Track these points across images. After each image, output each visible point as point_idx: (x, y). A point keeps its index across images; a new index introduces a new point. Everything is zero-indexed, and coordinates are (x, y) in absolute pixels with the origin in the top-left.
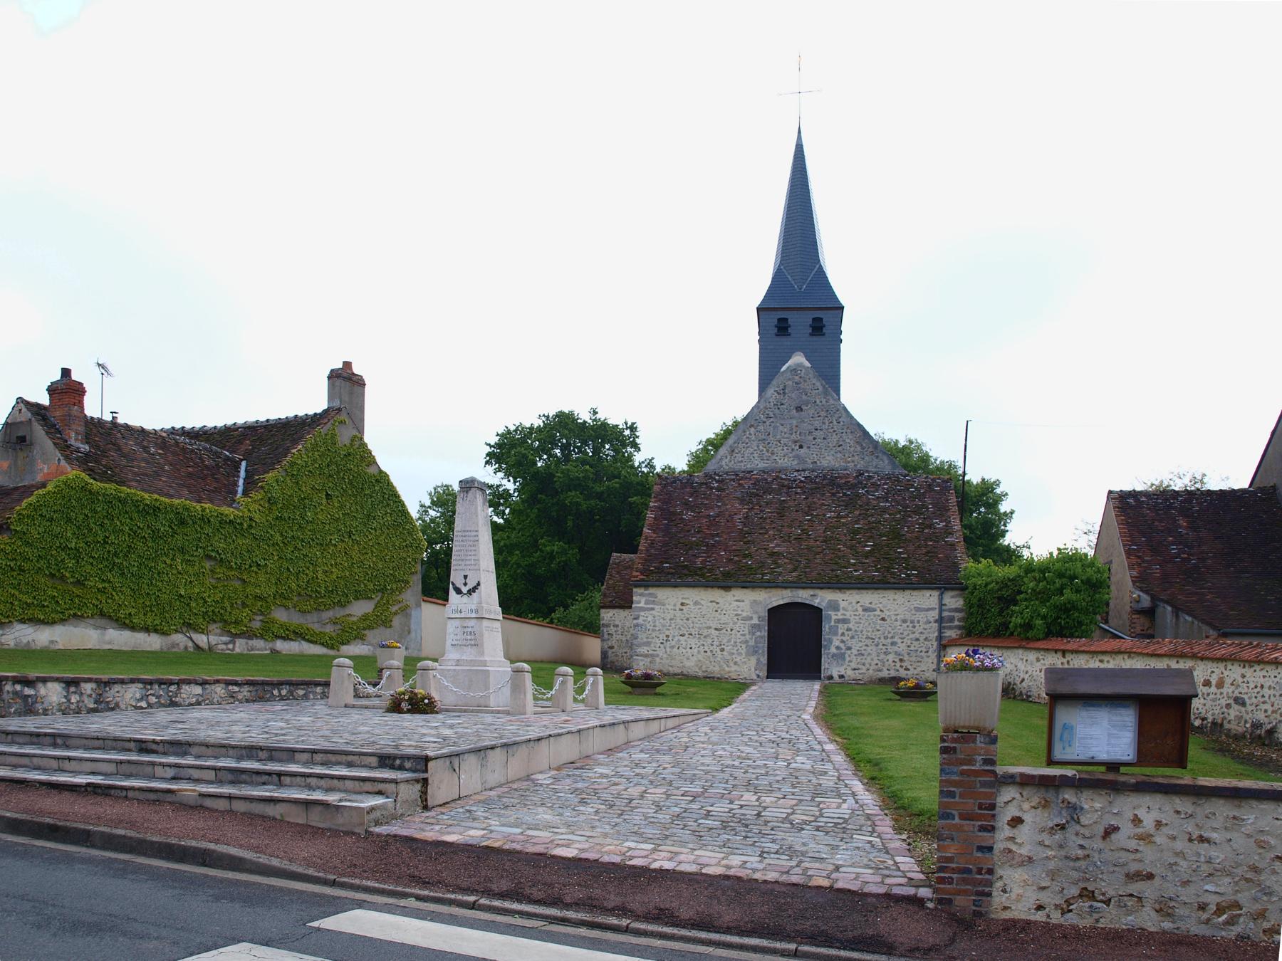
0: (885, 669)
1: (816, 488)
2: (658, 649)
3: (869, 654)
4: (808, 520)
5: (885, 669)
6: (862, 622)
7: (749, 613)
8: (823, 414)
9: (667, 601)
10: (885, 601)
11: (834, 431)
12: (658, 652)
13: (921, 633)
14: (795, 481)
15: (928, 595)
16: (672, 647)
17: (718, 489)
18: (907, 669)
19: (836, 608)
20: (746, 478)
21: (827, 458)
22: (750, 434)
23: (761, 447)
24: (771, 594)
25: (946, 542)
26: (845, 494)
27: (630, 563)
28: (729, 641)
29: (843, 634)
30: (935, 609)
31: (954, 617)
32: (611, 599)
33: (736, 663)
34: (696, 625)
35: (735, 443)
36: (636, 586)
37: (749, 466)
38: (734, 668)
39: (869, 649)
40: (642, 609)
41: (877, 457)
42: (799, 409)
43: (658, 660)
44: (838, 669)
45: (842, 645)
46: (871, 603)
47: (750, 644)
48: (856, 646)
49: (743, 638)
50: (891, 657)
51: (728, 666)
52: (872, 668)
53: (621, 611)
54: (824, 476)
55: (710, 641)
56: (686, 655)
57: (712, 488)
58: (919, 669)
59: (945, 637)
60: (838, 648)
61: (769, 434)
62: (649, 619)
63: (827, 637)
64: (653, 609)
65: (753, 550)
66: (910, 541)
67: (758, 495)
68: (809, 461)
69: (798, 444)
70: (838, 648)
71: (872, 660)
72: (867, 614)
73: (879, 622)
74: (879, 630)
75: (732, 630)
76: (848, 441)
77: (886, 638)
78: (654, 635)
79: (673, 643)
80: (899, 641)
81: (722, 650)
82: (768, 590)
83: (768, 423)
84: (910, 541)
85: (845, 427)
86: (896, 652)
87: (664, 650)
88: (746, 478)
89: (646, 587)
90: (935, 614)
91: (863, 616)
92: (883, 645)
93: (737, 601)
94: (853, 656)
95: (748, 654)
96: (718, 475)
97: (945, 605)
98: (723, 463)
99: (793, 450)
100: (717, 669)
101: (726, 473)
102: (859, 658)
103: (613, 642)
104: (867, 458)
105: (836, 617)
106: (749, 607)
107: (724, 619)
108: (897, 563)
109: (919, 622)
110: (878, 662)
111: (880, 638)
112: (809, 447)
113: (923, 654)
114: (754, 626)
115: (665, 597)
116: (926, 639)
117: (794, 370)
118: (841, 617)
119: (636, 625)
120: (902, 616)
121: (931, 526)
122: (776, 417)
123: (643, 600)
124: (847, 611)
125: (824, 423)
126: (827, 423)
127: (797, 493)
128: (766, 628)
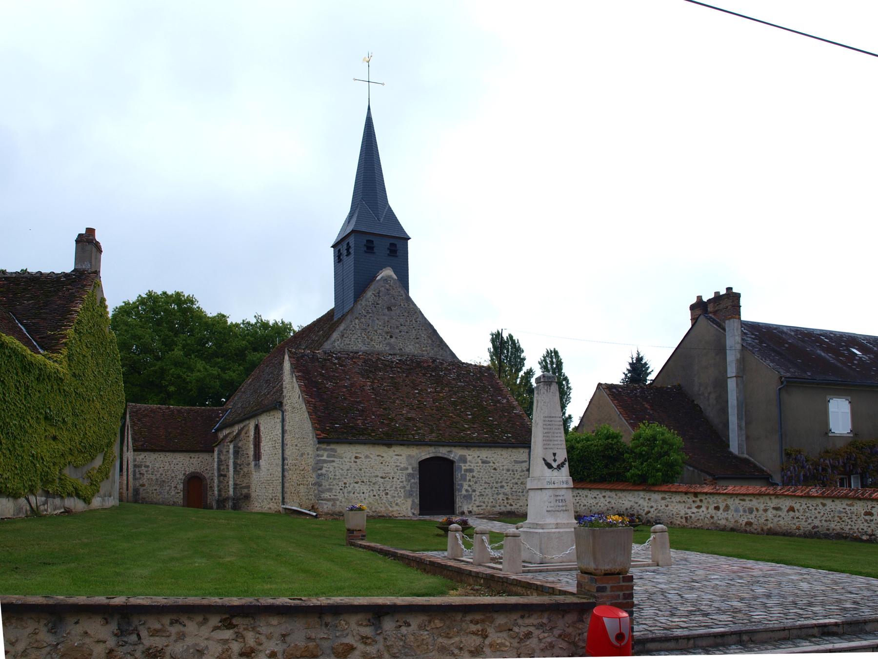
0: (497, 505)
3: (487, 495)
5: (497, 505)
6: (482, 471)
7: (405, 465)
10: (496, 456)
11: (414, 328)
12: (338, 497)
13: (519, 479)
15: (522, 452)
16: (349, 492)
18: (511, 505)
19: (465, 461)
21: (409, 347)
22: (355, 324)
23: (363, 334)
24: (421, 450)
27: (146, 412)
28: (392, 487)
29: (470, 480)
30: (525, 462)
32: (141, 443)
33: (397, 504)
34: (367, 474)
35: (344, 330)
37: (354, 348)
38: (396, 508)
39: (487, 491)
41: (442, 349)
42: (389, 309)
43: (338, 503)
45: (469, 489)
46: (487, 458)
47: (407, 489)
48: (479, 489)
50: (501, 497)
51: (391, 506)
52: (489, 505)
53: (152, 454)
55: (377, 487)
56: (360, 499)
58: (518, 505)
60: (467, 491)
61: (369, 326)
64: (333, 461)
68: (397, 348)
70: (467, 491)
71: (489, 499)
72: (485, 465)
73: (493, 471)
74: (492, 477)
75: (393, 478)
76: (423, 335)
77: (497, 483)
78: (334, 482)
79: (350, 489)
80: (505, 485)
81: (387, 494)
82: (419, 447)
83: (368, 317)
85: (421, 325)
89: (329, 443)
91: (482, 466)
92: (496, 488)
93: (396, 455)
95: (406, 497)
98: (336, 344)
99: (385, 338)
100: (383, 509)
101: (339, 352)
103: (144, 480)
104: (435, 349)
106: (405, 459)
107: (387, 469)
109: (517, 471)
110: (492, 500)
111: (493, 483)
112: (396, 338)
113: (520, 494)
114: (409, 475)
115: (342, 452)
117: (386, 280)
118: (468, 468)
119: (322, 475)
120: (507, 467)
121: (499, 401)
123: (326, 454)
124: (472, 463)
125: (406, 321)
127: (399, 372)
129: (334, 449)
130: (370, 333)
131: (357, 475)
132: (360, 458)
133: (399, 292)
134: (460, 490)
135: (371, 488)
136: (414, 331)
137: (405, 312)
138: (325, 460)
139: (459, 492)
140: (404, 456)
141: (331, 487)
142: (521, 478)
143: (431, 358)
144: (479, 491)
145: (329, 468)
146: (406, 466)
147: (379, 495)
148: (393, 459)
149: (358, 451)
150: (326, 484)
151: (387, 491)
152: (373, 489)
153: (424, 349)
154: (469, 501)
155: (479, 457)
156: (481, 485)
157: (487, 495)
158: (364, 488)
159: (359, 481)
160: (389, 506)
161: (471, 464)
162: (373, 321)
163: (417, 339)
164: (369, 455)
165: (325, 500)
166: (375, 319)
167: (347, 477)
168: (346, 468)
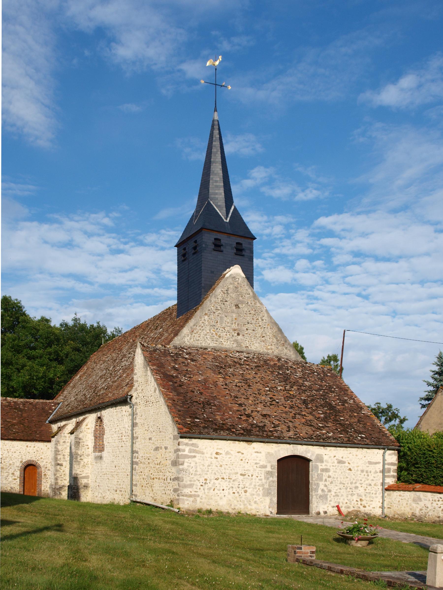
0: (351, 506)
3: (342, 495)
9: (205, 451)
11: (260, 326)
13: (373, 480)
14: (240, 359)
16: (209, 489)
17: (192, 360)
18: (365, 507)
20: (206, 354)
21: (255, 345)
22: (204, 320)
23: (212, 331)
28: (251, 484)
29: (326, 480)
30: (379, 463)
31: (390, 468)
33: (255, 502)
34: (226, 471)
35: (194, 325)
37: (203, 344)
39: (342, 491)
40: (186, 457)
41: (286, 348)
42: (237, 306)
43: (198, 499)
44: (323, 506)
45: (325, 489)
48: (334, 489)
51: (250, 504)
55: (236, 483)
56: (220, 495)
57: (186, 358)
58: (371, 506)
59: (386, 483)
61: (217, 322)
63: (316, 482)
64: (195, 457)
67: (221, 367)
68: (244, 346)
69: (236, 332)
70: (323, 490)
71: (344, 499)
72: (340, 465)
74: (347, 478)
75: (252, 476)
76: (268, 334)
77: (351, 483)
78: (195, 478)
79: (210, 485)
80: (359, 486)
81: (246, 492)
83: (216, 314)
86: (358, 494)
87: (203, 491)
90: (380, 467)
92: (350, 489)
94: (332, 497)
95: (264, 495)
102: (336, 498)
104: (280, 348)
107: (247, 466)
109: (370, 472)
112: (243, 335)
113: (373, 495)
114: (268, 473)
116: (375, 485)
117: (233, 277)
118: (324, 467)
121: (345, 401)
122: (222, 310)
123: (187, 449)
126: (255, 319)
127: (247, 369)
128: (276, 474)
129: (195, 444)
130: (218, 330)
131: (217, 471)
132: (221, 454)
133: (247, 290)
134: (316, 490)
135: (231, 485)
136: (260, 329)
137: (252, 310)
140: (263, 454)
141: (192, 482)
143: (277, 357)
145: (190, 463)
146: (265, 464)
147: (238, 492)
149: (219, 447)
150: (187, 480)
151: (246, 489)
152: (233, 486)
153: (269, 347)
154: (324, 501)
156: (336, 486)
157: (342, 495)
158: (224, 484)
160: (248, 504)
162: (221, 318)
164: (230, 451)
165: (186, 496)
166: (223, 316)
167: (208, 473)
168: (207, 464)
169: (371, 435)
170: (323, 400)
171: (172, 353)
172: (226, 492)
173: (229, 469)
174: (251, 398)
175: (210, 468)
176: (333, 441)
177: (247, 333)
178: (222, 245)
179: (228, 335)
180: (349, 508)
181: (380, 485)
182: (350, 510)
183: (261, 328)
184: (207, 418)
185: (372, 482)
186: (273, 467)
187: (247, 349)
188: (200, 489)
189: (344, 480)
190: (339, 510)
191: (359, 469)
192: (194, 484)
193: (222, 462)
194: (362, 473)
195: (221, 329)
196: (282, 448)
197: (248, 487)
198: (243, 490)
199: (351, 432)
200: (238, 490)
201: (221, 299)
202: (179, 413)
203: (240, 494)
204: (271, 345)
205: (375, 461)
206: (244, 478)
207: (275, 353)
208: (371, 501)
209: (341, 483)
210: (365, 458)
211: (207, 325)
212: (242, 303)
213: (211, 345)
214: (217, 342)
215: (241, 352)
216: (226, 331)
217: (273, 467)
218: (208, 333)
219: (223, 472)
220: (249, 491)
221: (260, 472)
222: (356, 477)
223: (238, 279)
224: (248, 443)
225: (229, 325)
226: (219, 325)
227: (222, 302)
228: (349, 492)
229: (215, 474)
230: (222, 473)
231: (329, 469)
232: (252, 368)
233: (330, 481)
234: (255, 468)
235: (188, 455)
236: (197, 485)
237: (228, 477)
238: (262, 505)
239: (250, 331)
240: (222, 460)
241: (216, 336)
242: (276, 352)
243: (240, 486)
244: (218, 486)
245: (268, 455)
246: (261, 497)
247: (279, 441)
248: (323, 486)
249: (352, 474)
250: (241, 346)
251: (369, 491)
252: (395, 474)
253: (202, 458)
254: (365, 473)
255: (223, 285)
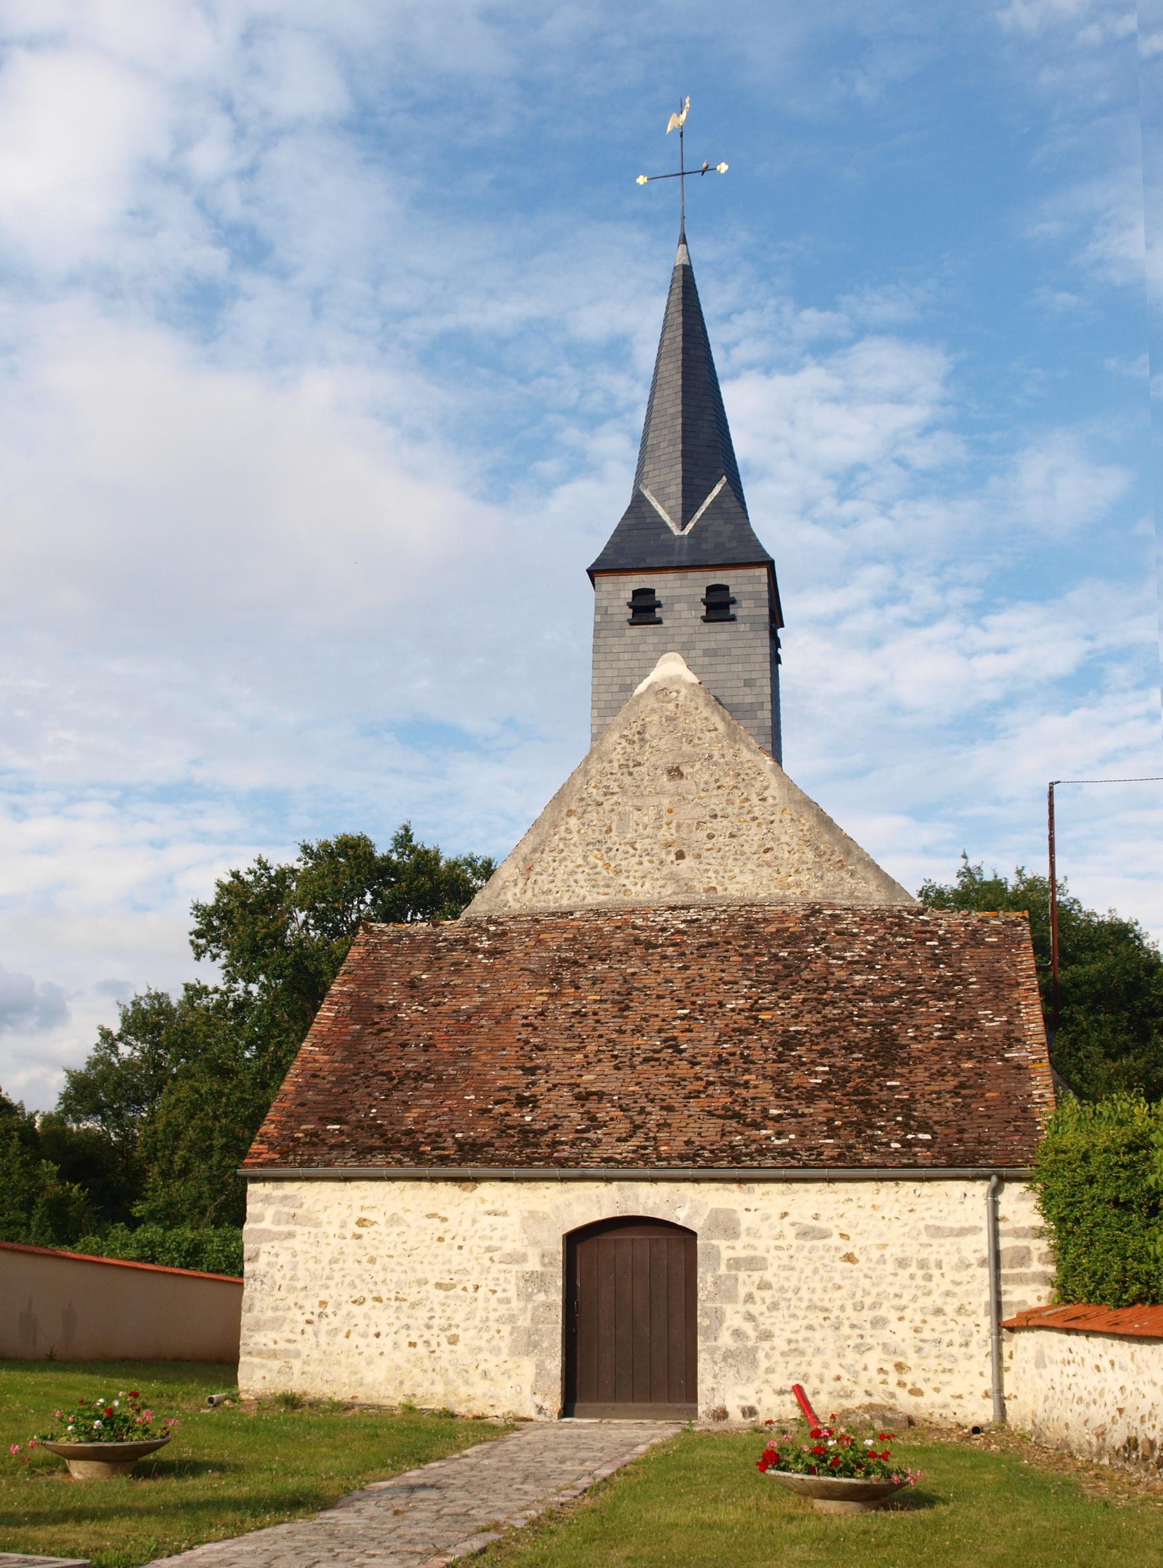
1: (710, 945)
2: (298, 1337)
3: (818, 1350)
4: (683, 1018)
8: (728, 781)
9: (323, 1217)
10: (851, 1210)
11: (754, 819)
12: (299, 1346)
13: (948, 1294)
14: (663, 930)
16: (334, 1332)
17: (492, 953)
18: (916, 1392)
21: (740, 878)
22: (568, 831)
23: (591, 859)
25: (1007, 1060)
26: (775, 958)
29: (750, 1298)
30: (974, 1230)
34: (389, 1276)
35: (534, 851)
36: (255, 1179)
39: (818, 1335)
40: (268, 1236)
41: (853, 874)
42: (675, 773)
43: (297, 1365)
44: (740, 1390)
45: (748, 1328)
46: (816, 1217)
48: (783, 1329)
49: (503, 1310)
50: (874, 1359)
51: (466, 1382)
54: (731, 917)
55: (422, 1314)
56: (367, 1352)
57: (476, 951)
58: (947, 1391)
59: (1011, 1304)
60: (737, 1333)
61: (609, 830)
62: (281, 1260)
63: (709, 1305)
64: (291, 1235)
65: (542, 1086)
66: (919, 1060)
67: (575, 963)
68: (699, 887)
69: (674, 850)
70: (737, 1333)
71: (826, 1365)
72: (809, 1244)
74: (839, 1287)
76: (785, 839)
77: (859, 1307)
79: (336, 1322)
80: (893, 1316)
84: (919, 1060)
86: (885, 1345)
87: (313, 1339)
88: (556, 928)
90: (982, 1243)
92: (853, 1326)
94: (776, 1355)
95: (515, 1351)
96: (495, 923)
97: (1004, 1219)
98: (509, 897)
100: (439, 1389)
102: (794, 1360)
104: (829, 876)
105: (731, 1254)
107: (458, 1259)
108: (881, 1114)
109: (939, 1265)
110: (838, 1371)
112: (699, 856)
114: (530, 1278)
116: (960, 1310)
117: (661, 692)
118: (742, 1253)
121: (971, 1024)
123: (270, 1213)
126: (737, 801)
127: (664, 957)
128: (560, 1283)
129: (294, 1197)
131: (360, 1276)
133: (706, 719)
135: (404, 1320)
136: (754, 830)
137: (726, 775)
138: (264, 1230)
139: (707, 1339)
140: (515, 1217)
141: (280, 1313)
142: (956, 1289)
144: (788, 1335)
146: (522, 1250)
147: (427, 1342)
148: (477, 1226)
149: (367, 1203)
151: (454, 1331)
152: (410, 1322)
153: (791, 879)
155: (785, 1214)
156: (794, 1316)
158: (382, 1317)
159: (369, 1297)
160: (460, 1381)
161: (754, 1242)
163: (766, 851)
164: (401, 1214)
167: (332, 1283)
168: (329, 1257)
169: (962, 1131)
170: (875, 1025)
171: (445, 940)
172: (386, 1342)
173: (399, 1269)
174: (591, 1048)
175: (336, 1267)
176: (769, 1162)
177: (709, 846)
178: (659, 605)
179: (646, 864)
180: (849, 1395)
181: (981, 1311)
182: (849, 1404)
183: (759, 825)
184: (374, 1119)
185: (949, 1300)
186: (546, 1260)
187: (712, 894)
188: (303, 1332)
189: (827, 1297)
190: (804, 1403)
191: (887, 1253)
192: (284, 1319)
193: (377, 1248)
194: (900, 1271)
195: (622, 848)
196: (578, 1197)
197: (462, 1325)
198: (443, 1335)
199: (880, 1128)
200: (427, 1335)
201: (622, 762)
202: (300, 1109)
203: (434, 1346)
204: (797, 871)
205: (957, 1225)
206: (447, 1297)
207: (812, 894)
208: (944, 1371)
209: (811, 1307)
210: (914, 1216)
211: (575, 845)
212: (691, 762)
213: (589, 900)
214: (607, 890)
215: (683, 908)
216: (638, 853)
217: (546, 1260)
218: (579, 866)
219: (379, 1278)
220: (465, 1337)
221: (502, 1276)
222: (874, 1285)
223: (678, 692)
224: (464, 1185)
225: (649, 831)
226: (615, 839)
227: (625, 770)
228: (849, 1337)
229: (353, 1285)
230: (376, 1283)
231: (764, 1259)
232: (684, 954)
233: (768, 1301)
234: (487, 1263)
235: (270, 1231)
236: (293, 1321)
237: (393, 1296)
238: (510, 1383)
239: (720, 840)
240: (376, 1242)
241: (605, 873)
242: (816, 892)
243: (436, 1322)
244: (362, 1323)
245: (531, 1221)
246: (504, 1357)
247: (558, 1172)
248: (738, 1316)
249: (861, 1275)
250: (690, 889)
251: (936, 1335)
252: (1051, 1269)
253: (311, 1240)
254: (913, 1269)
255: (627, 719)
